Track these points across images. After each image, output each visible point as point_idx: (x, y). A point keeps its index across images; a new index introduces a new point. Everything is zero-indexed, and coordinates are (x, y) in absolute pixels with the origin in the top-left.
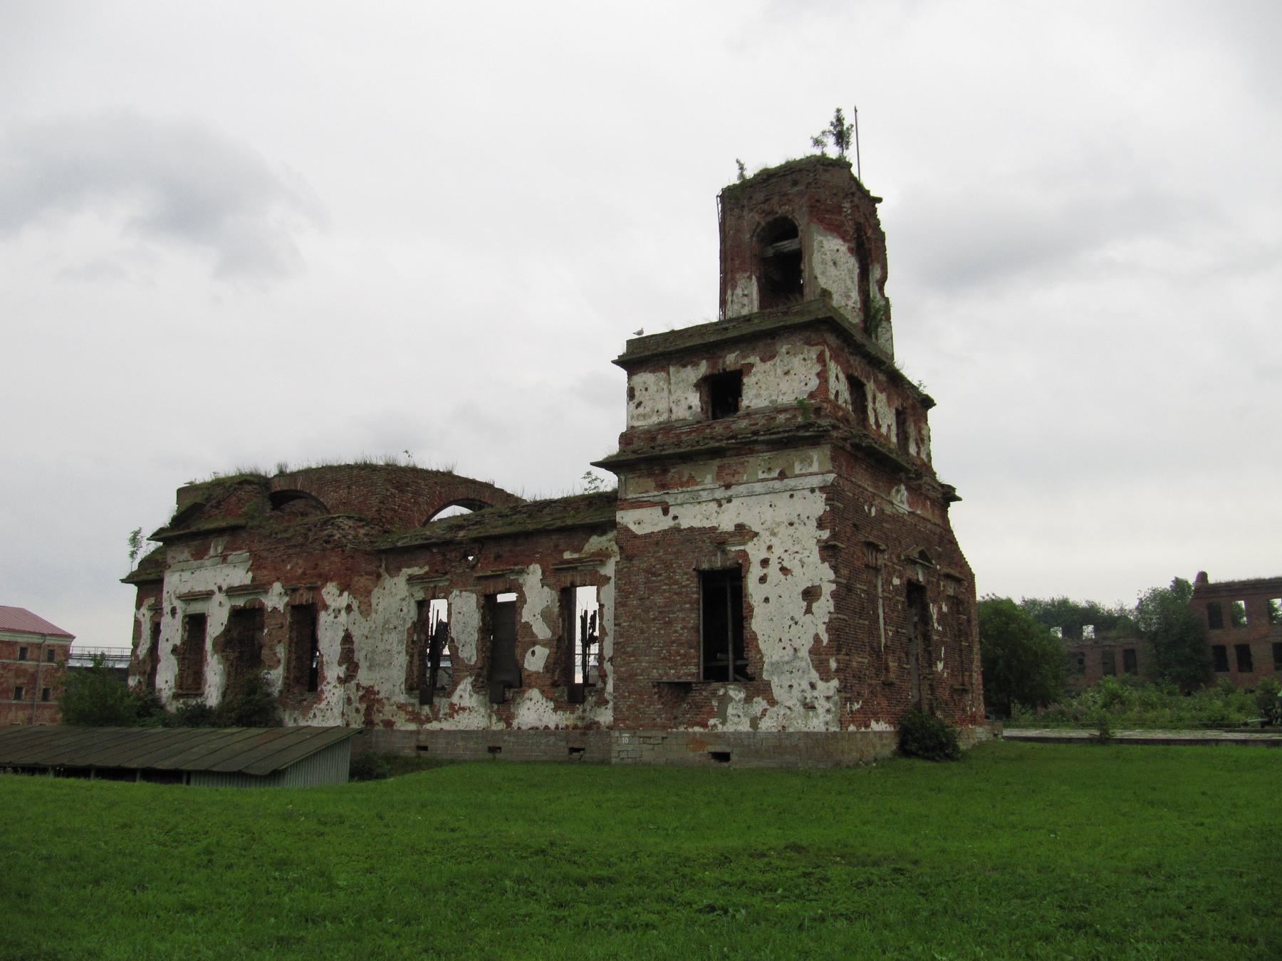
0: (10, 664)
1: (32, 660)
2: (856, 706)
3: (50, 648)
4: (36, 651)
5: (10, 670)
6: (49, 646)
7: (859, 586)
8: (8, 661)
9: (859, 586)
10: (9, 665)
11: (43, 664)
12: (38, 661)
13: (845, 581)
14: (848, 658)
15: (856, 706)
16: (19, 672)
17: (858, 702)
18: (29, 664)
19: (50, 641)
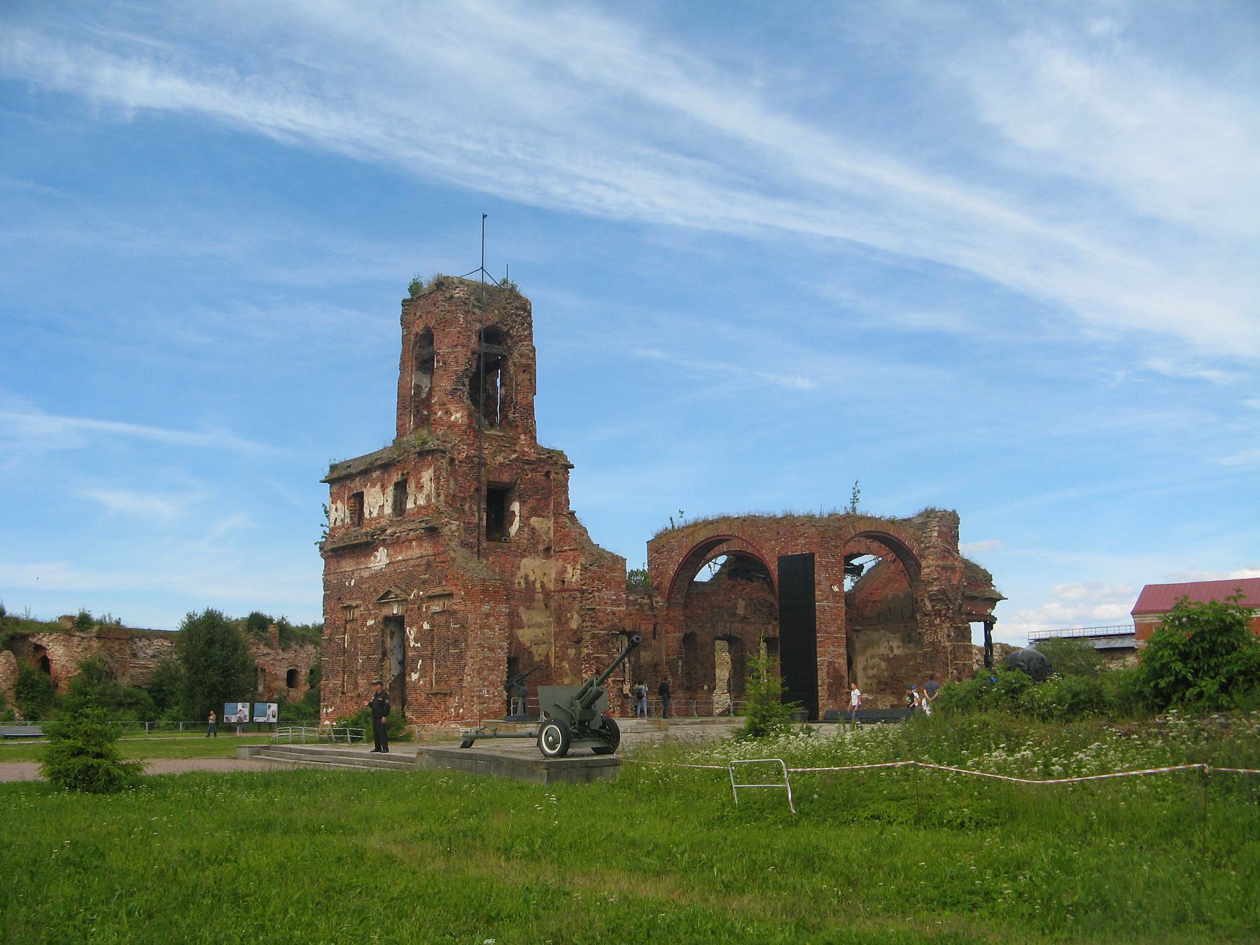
2: (330, 710)
13: (328, 637)
15: (330, 710)
17: (331, 708)
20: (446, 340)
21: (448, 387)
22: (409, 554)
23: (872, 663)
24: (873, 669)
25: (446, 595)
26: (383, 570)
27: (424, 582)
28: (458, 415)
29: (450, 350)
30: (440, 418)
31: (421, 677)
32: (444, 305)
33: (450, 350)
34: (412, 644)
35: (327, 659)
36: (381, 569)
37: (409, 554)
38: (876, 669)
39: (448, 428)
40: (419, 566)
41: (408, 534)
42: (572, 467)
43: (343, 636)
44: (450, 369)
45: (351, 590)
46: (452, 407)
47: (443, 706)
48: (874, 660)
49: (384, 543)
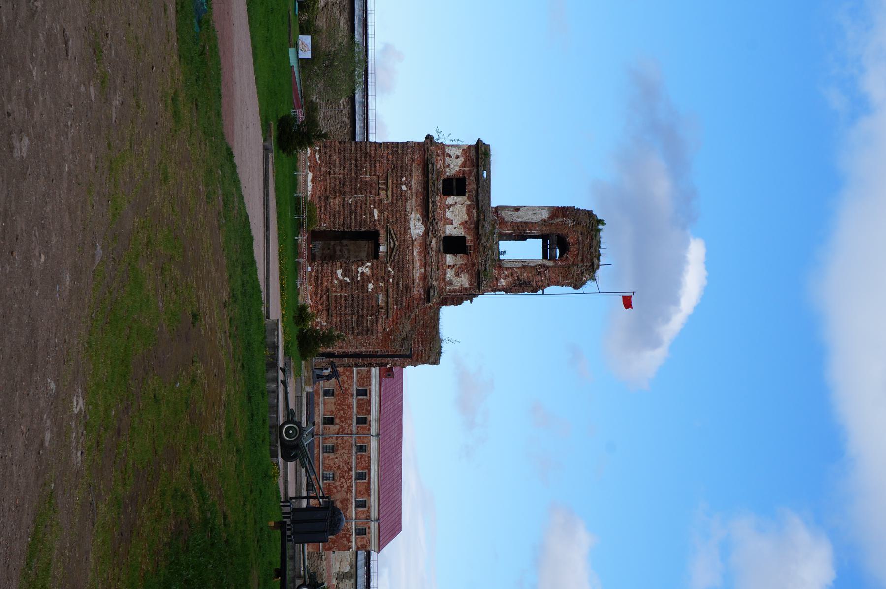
0: (352, 493)
1: (356, 513)
3: (367, 531)
4: (364, 516)
5: (347, 493)
6: (369, 528)
7: (368, 166)
8: (354, 491)
9: (368, 166)
10: (351, 491)
11: (354, 524)
12: (356, 519)
14: (337, 151)
15: (318, 156)
16: (345, 502)
18: (353, 511)
19: (373, 526)
20: (554, 275)
21: (523, 277)
22: (418, 264)
23: (344, 250)
24: (340, 251)
25: (388, 316)
26: (409, 231)
27: (397, 284)
28: (503, 284)
29: (547, 277)
30: (503, 273)
31: (340, 281)
32: (578, 271)
33: (547, 277)
34: (360, 270)
35: (353, 152)
36: (409, 228)
37: (418, 264)
38: (340, 253)
39: (496, 278)
40: (408, 277)
41: (429, 266)
42: (471, 302)
43: (368, 173)
44: (534, 278)
45: (398, 185)
46: (509, 280)
47: (321, 307)
48: (346, 252)
49: (426, 234)
